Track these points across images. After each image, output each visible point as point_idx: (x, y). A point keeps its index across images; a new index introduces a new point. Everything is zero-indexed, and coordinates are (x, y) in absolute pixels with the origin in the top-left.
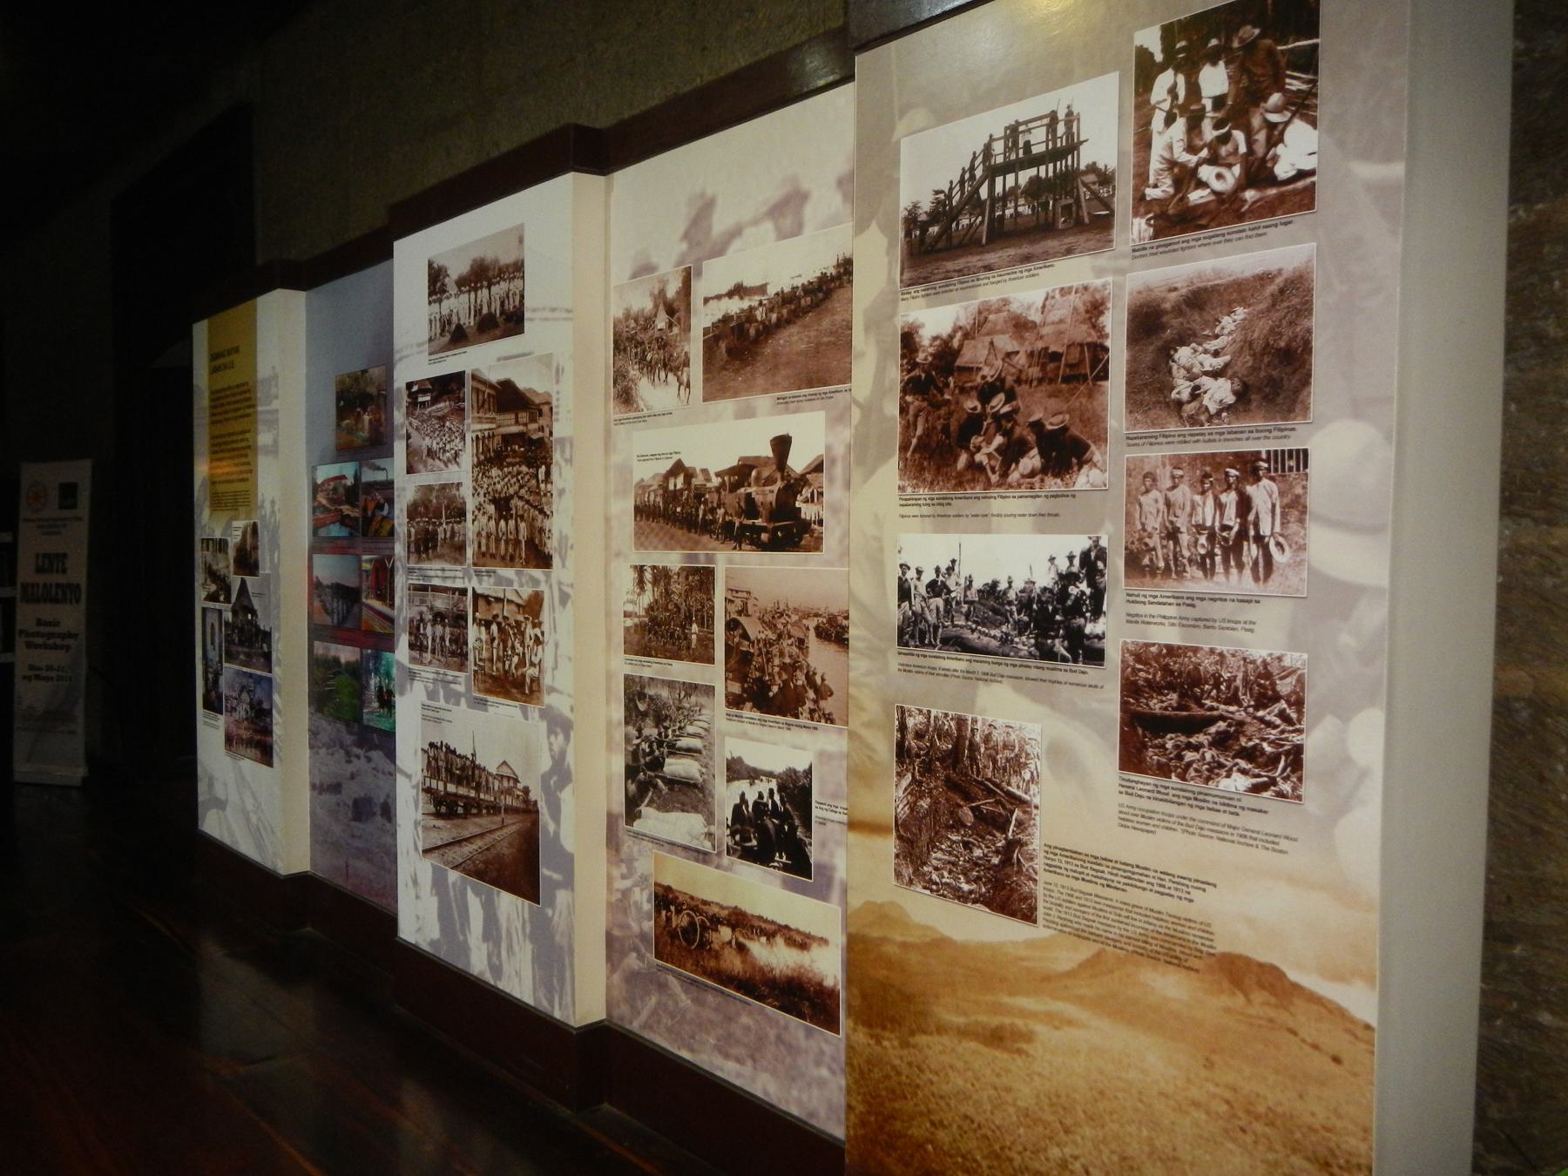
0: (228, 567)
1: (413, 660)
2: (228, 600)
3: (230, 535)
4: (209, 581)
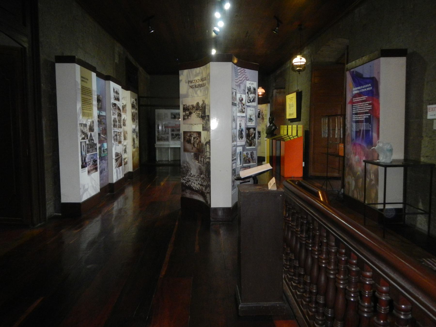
0: (87, 130)
1: (114, 142)
2: (87, 138)
3: (88, 123)
4: (82, 135)
